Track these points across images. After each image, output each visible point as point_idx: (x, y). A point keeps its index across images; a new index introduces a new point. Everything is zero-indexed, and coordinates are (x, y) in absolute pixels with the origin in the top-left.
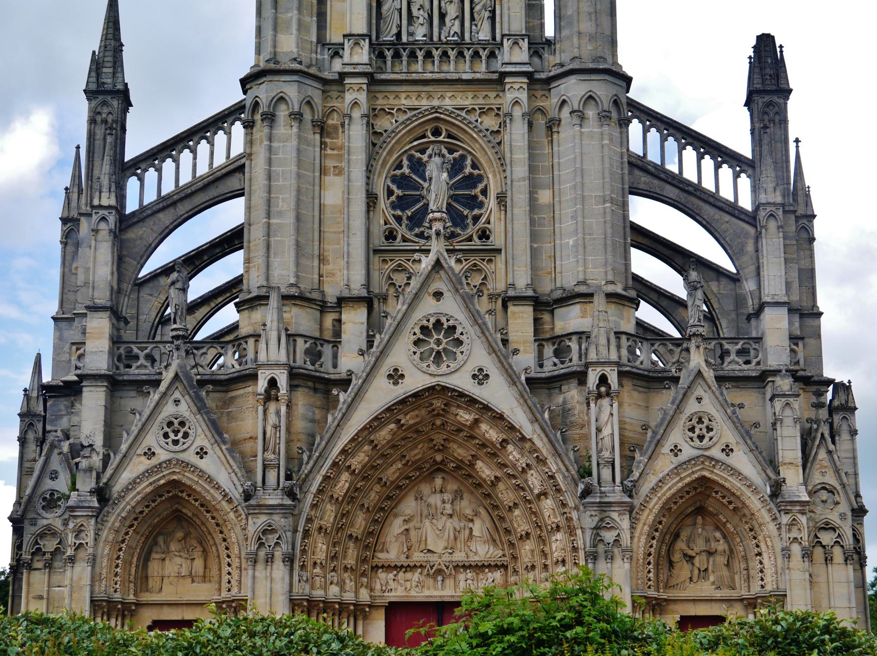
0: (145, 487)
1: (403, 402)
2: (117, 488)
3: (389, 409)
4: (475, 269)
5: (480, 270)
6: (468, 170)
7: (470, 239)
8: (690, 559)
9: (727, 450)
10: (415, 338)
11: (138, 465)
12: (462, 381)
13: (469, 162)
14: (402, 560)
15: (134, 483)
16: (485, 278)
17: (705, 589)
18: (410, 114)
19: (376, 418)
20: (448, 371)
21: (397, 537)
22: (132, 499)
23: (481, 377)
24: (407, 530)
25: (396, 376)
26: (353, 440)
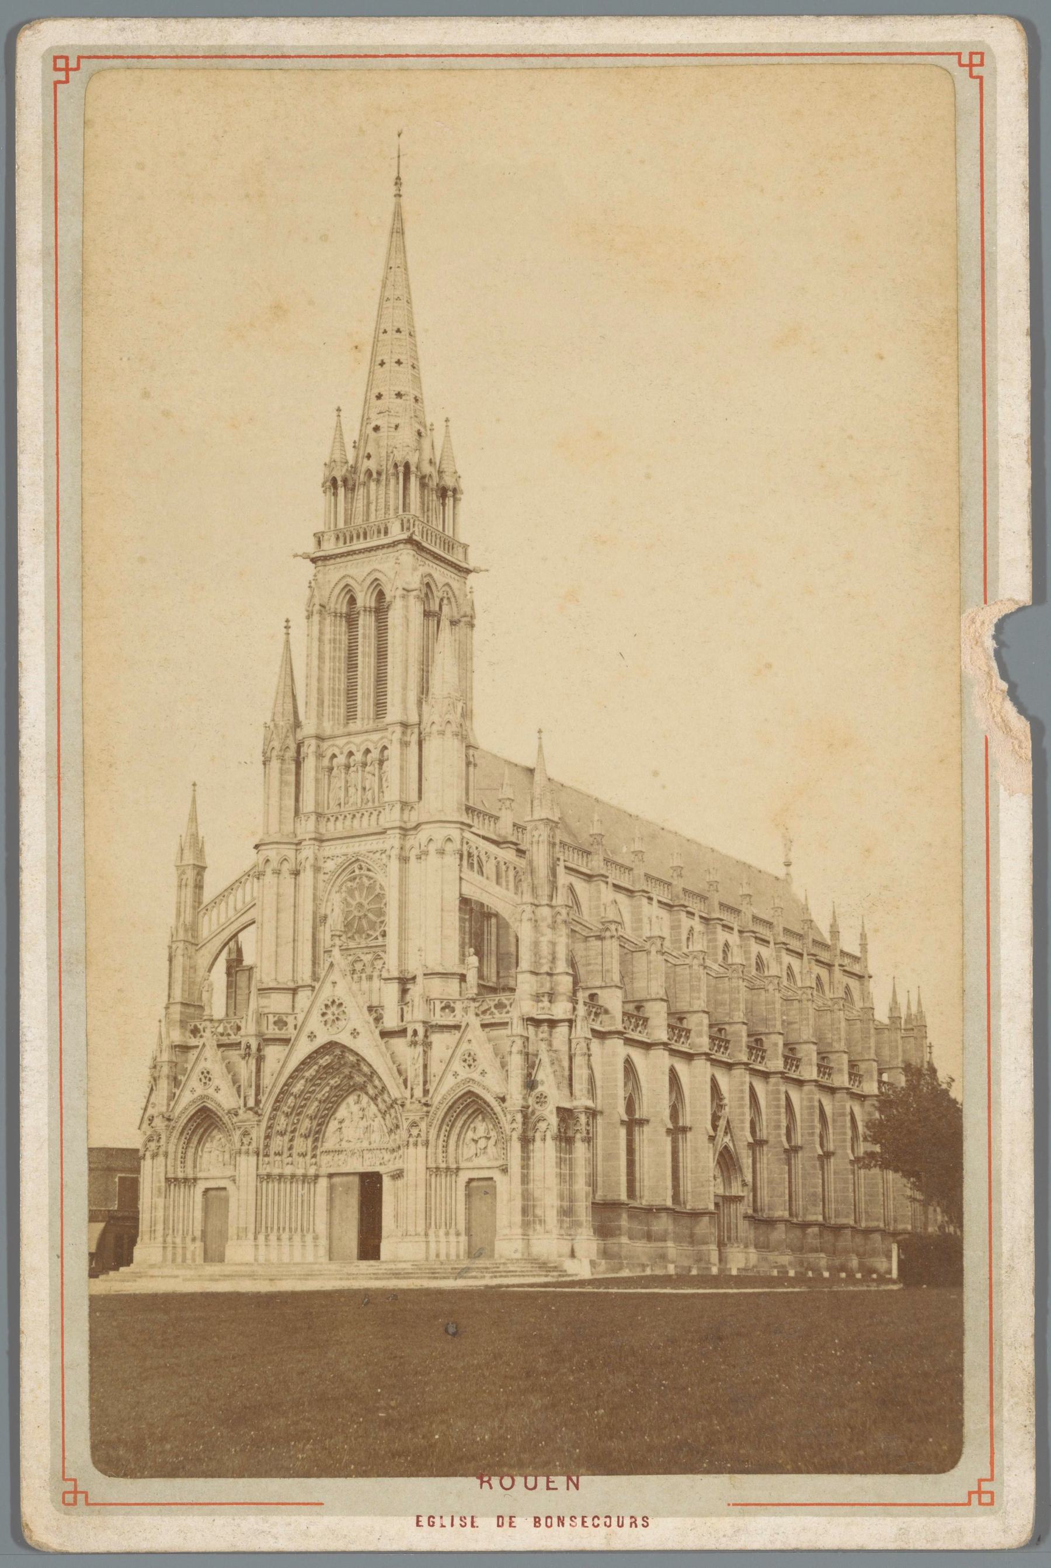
0: (192, 1110)
1: (316, 1052)
3: (309, 1057)
4: (378, 957)
5: (381, 958)
6: (378, 891)
7: (376, 938)
8: (476, 1141)
10: (321, 1012)
11: (186, 1098)
12: (344, 1038)
13: (378, 887)
14: (337, 1147)
16: (384, 963)
17: (482, 1161)
18: (344, 858)
19: (303, 1063)
21: (334, 1133)
22: (184, 1120)
23: (355, 1033)
24: (340, 1128)
26: (291, 1077)
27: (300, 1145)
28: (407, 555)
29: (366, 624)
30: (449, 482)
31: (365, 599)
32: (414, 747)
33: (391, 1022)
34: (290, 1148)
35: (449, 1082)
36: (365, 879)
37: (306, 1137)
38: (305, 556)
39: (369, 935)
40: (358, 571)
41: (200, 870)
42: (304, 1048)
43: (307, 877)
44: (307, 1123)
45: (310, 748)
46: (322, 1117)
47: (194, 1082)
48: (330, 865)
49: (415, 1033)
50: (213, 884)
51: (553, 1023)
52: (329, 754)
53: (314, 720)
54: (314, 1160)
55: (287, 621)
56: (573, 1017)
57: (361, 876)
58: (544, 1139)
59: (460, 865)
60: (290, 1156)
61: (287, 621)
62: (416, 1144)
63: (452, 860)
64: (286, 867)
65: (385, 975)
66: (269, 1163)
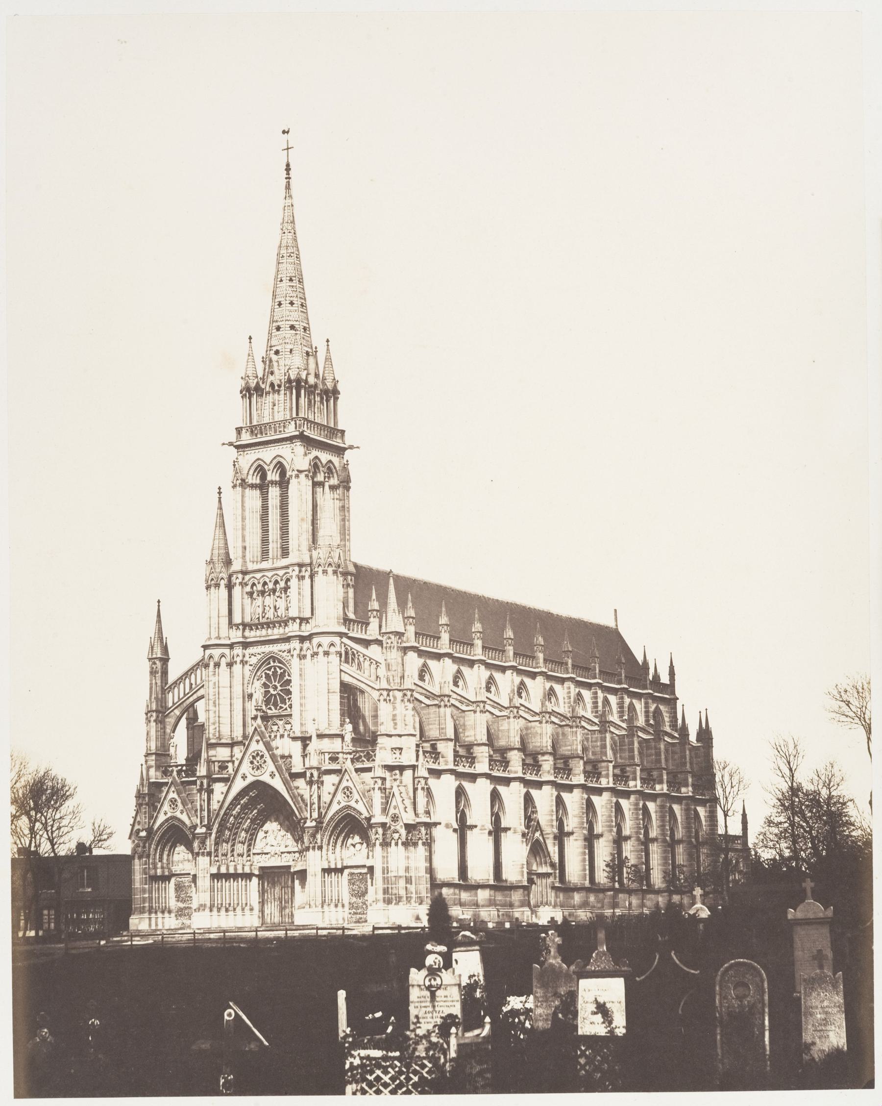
0: (165, 827)
2: (156, 827)
6: (287, 677)
7: (286, 709)
8: (354, 846)
9: (357, 802)
11: (162, 818)
12: (266, 778)
15: (161, 825)
18: (262, 655)
20: (261, 774)
23: (272, 775)
25: (244, 777)
27: (240, 848)
28: (299, 447)
29: (274, 493)
30: (330, 385)
31: (273, 476)
32: (307, 581)
33: (297, 768)
34: (233, 851)
35: (335, 808)
36: (278, 669)
37: (243, 843)
38: (231, 444)
39: (281, 707)
40: (267, 455)
41: (165, 660)
42: (239, 785)
43: (237, 668)
44: (243, 834)
45: (237, 579)
46: (253, 829)
47: (166, 807)
48: (254, 660)
49: (312, 775)
50: (174, 672)
51: (402, 768)
52: (250, 583)
53: (240, 561)
54: (249, 858)
55: (220, 488)
56: (416, 764)
57: (275, 667)
58: (397, 844)
59: (340, 660)
60: (233, 856)
61: (220, 488)
62: (314, 848)
63: (334, 659)
64: (223, 662)
65: (292, 735)
66: (218, 861)
